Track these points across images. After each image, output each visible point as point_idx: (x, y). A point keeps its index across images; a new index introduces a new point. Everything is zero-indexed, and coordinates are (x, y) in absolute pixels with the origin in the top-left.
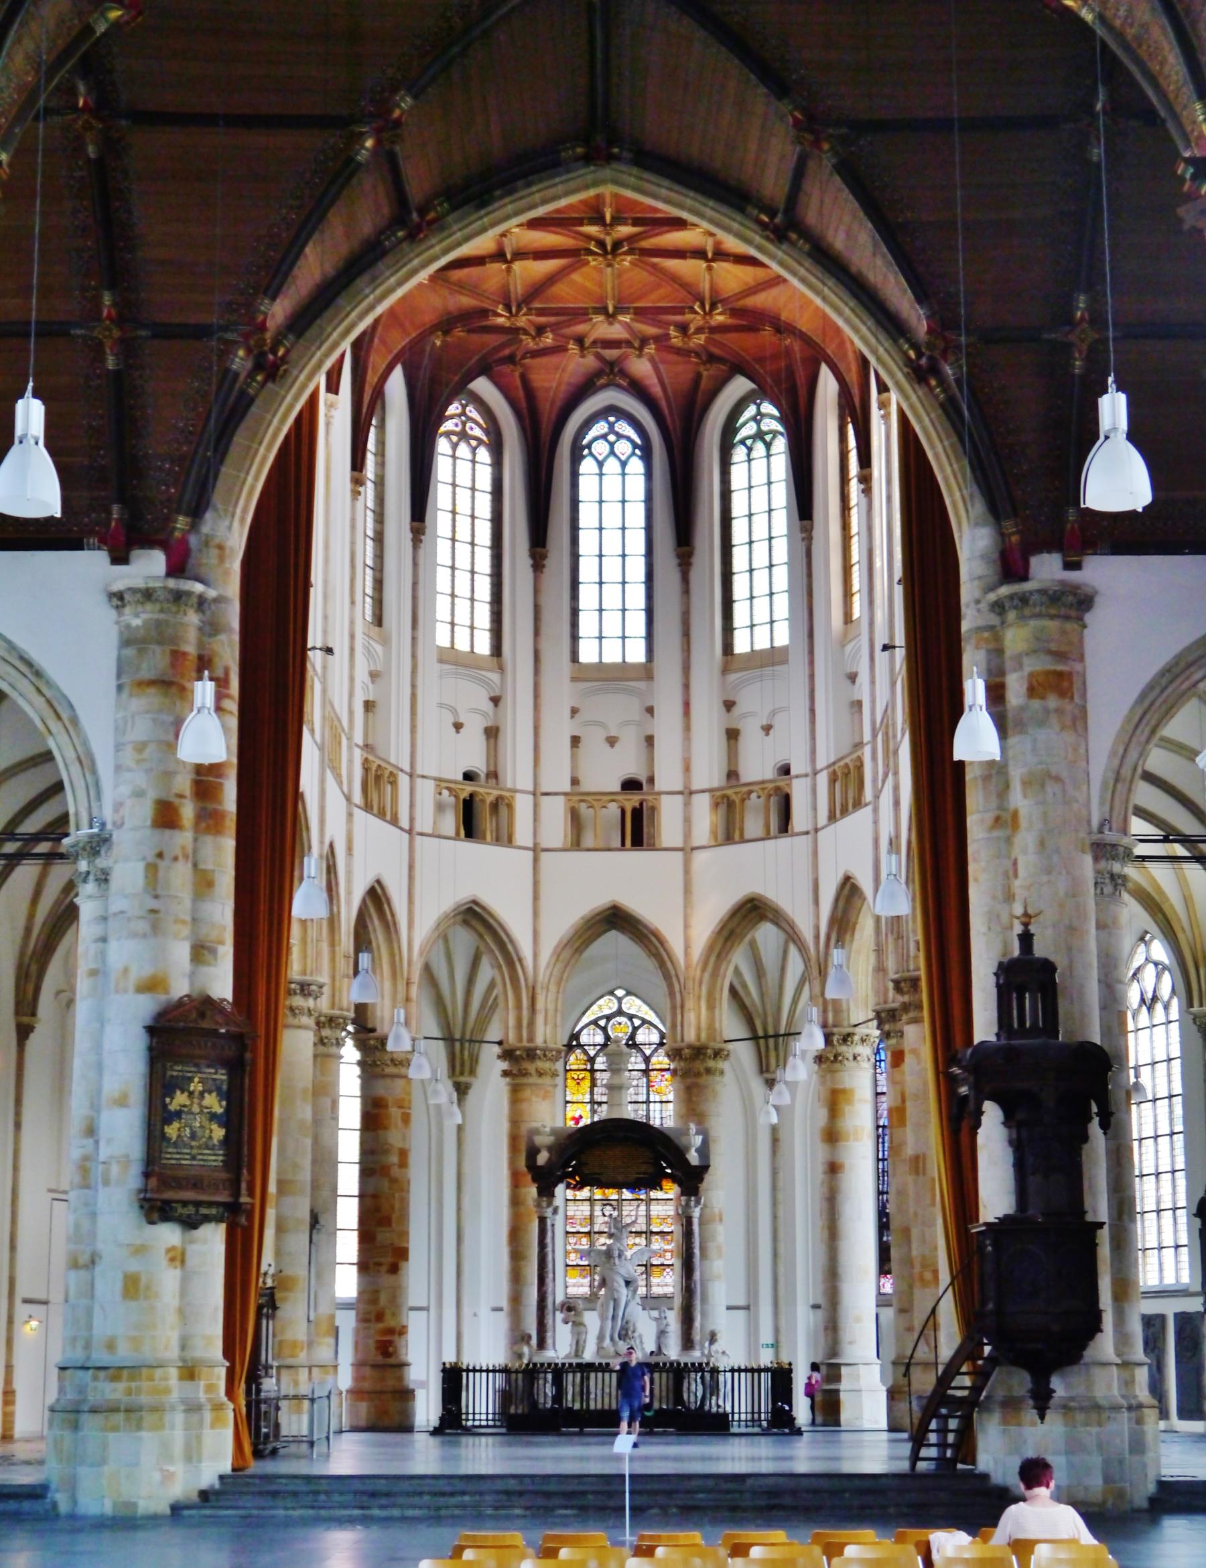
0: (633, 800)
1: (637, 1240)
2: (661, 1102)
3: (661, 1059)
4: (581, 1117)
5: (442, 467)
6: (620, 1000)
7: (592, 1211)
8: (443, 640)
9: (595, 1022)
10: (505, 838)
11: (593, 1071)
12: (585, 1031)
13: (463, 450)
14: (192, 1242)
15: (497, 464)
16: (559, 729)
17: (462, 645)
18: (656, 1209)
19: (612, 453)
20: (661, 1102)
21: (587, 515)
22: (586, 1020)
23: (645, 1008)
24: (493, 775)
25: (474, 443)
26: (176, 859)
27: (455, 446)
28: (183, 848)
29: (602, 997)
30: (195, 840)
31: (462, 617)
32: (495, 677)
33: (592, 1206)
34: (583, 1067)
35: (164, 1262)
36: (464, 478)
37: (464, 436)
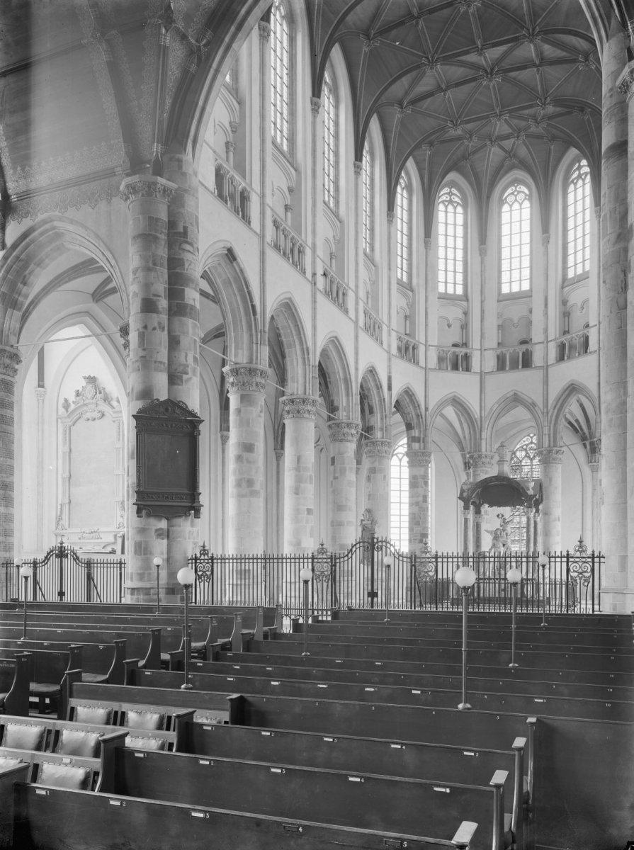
0: (524, 347)
5: (441, 216)
8: (441, 289)
10: (468, 369)
13: (450, 208)
15: (465, 213)
16: (492, 323)
17: (450, 291)
19: (516, 200)
21: (505, 230)
24: (465, 345)
25: (455, 205)
26: (154, 329)
27: (446, 207)
28: (160, 324)
31: (450, 279)
32: (465, 303)
36: (451, 220)
37: (451, 202)
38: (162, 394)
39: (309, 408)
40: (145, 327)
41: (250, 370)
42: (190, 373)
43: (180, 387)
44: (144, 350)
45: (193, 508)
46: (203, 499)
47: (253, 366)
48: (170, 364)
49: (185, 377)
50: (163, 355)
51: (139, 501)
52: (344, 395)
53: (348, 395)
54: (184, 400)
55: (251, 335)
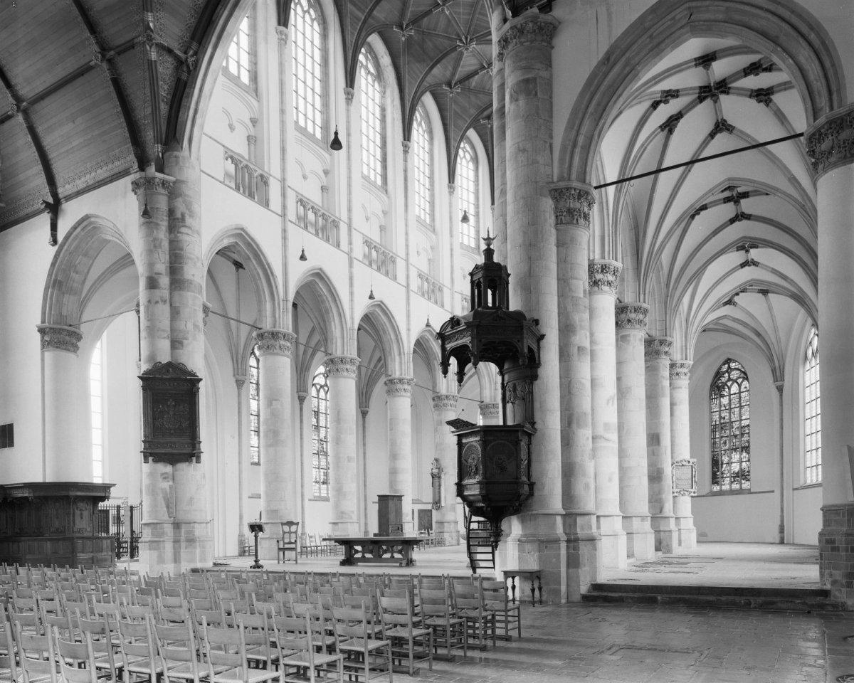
14: (176, 471)
26: (157, 302)
30: (171, 294)
35: (160, 480)
38: (165, 358)
39: (348, 367)
40: (149, 301)
41: (273, 334)
42: (190, 339)
43: (181, 351)
44: (148, 320)
45: (193, 455)
46: (203, 447)
47: (277, 329)
48: (172, 330)
49: (185, 342)
50: (165, 323)
51: (147, 449)
52: (396, 354)
53: (400, 354)
54: (180, 361)
55: (274, 304)
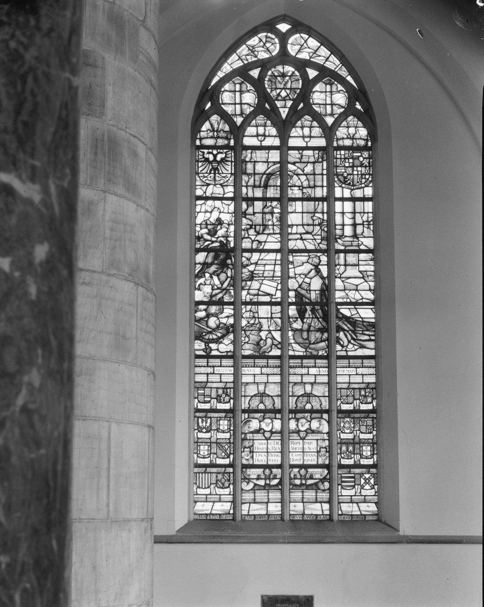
1: (315, 425)
2: (353, 199)
3: (352, 130)
4: (219, 222)
6: (284, 38)
7: (237, 375)
9: (242, 72)
11: (239, 148)
12: (227, 87)
18: (345, 375)
20: (353, 199)
22: (226, 68)
23: (324, 51)
29: (254, 32)
33: (236, 367)
34: (221, 142)
